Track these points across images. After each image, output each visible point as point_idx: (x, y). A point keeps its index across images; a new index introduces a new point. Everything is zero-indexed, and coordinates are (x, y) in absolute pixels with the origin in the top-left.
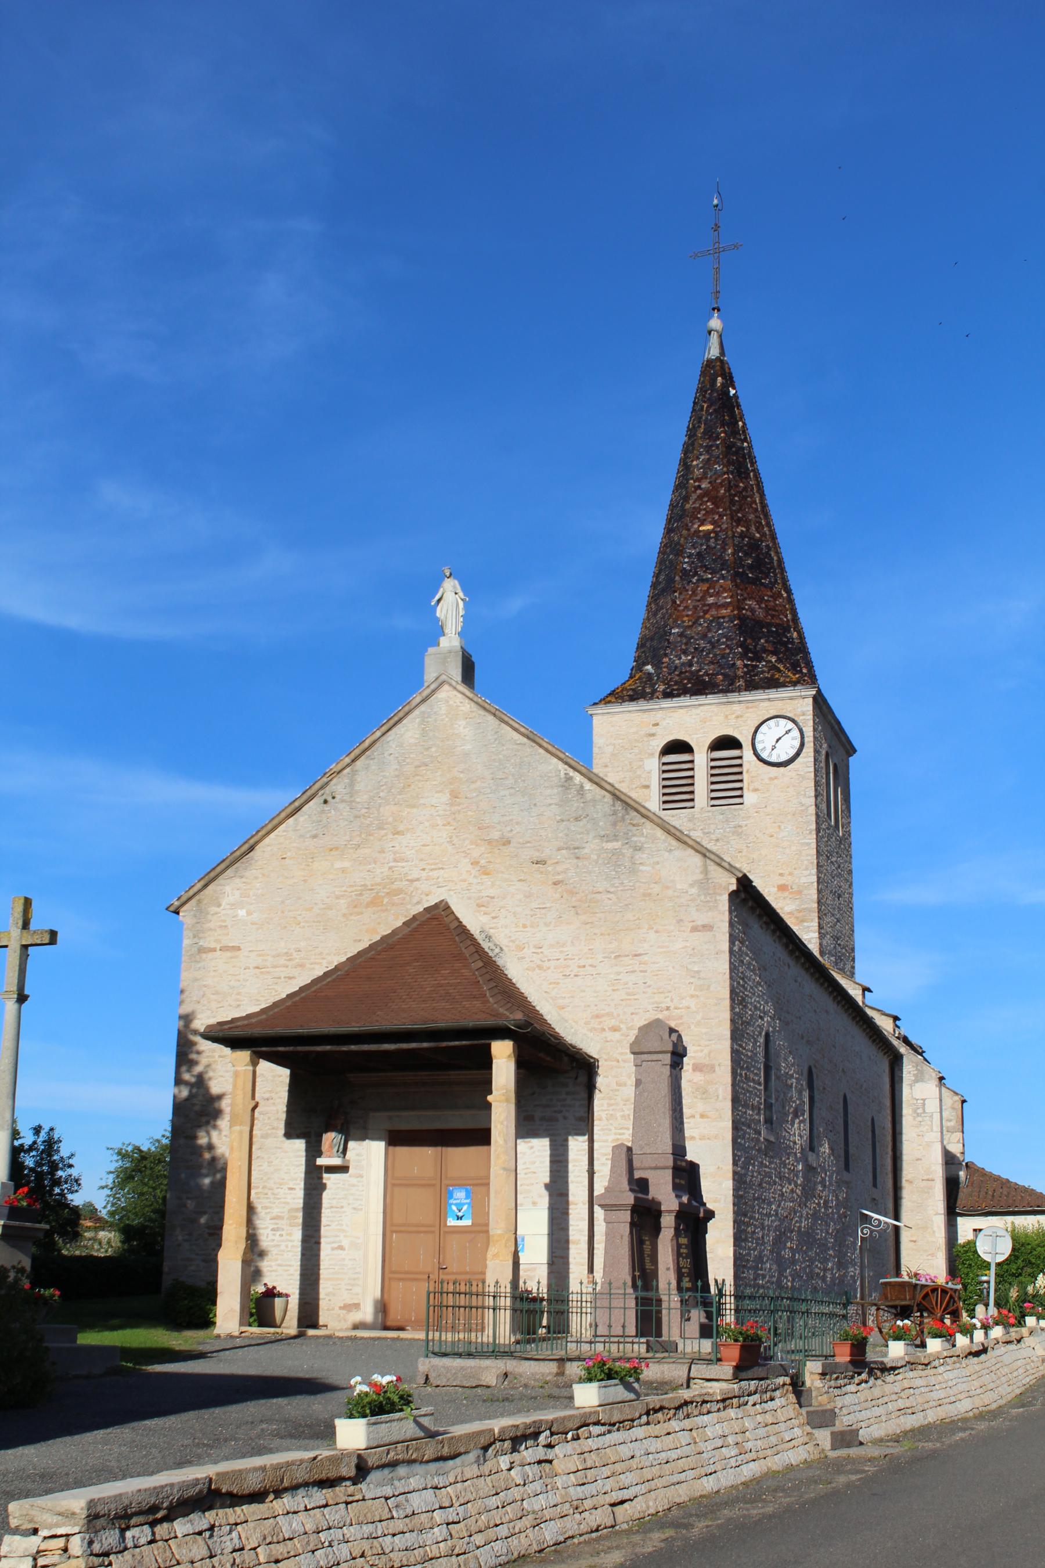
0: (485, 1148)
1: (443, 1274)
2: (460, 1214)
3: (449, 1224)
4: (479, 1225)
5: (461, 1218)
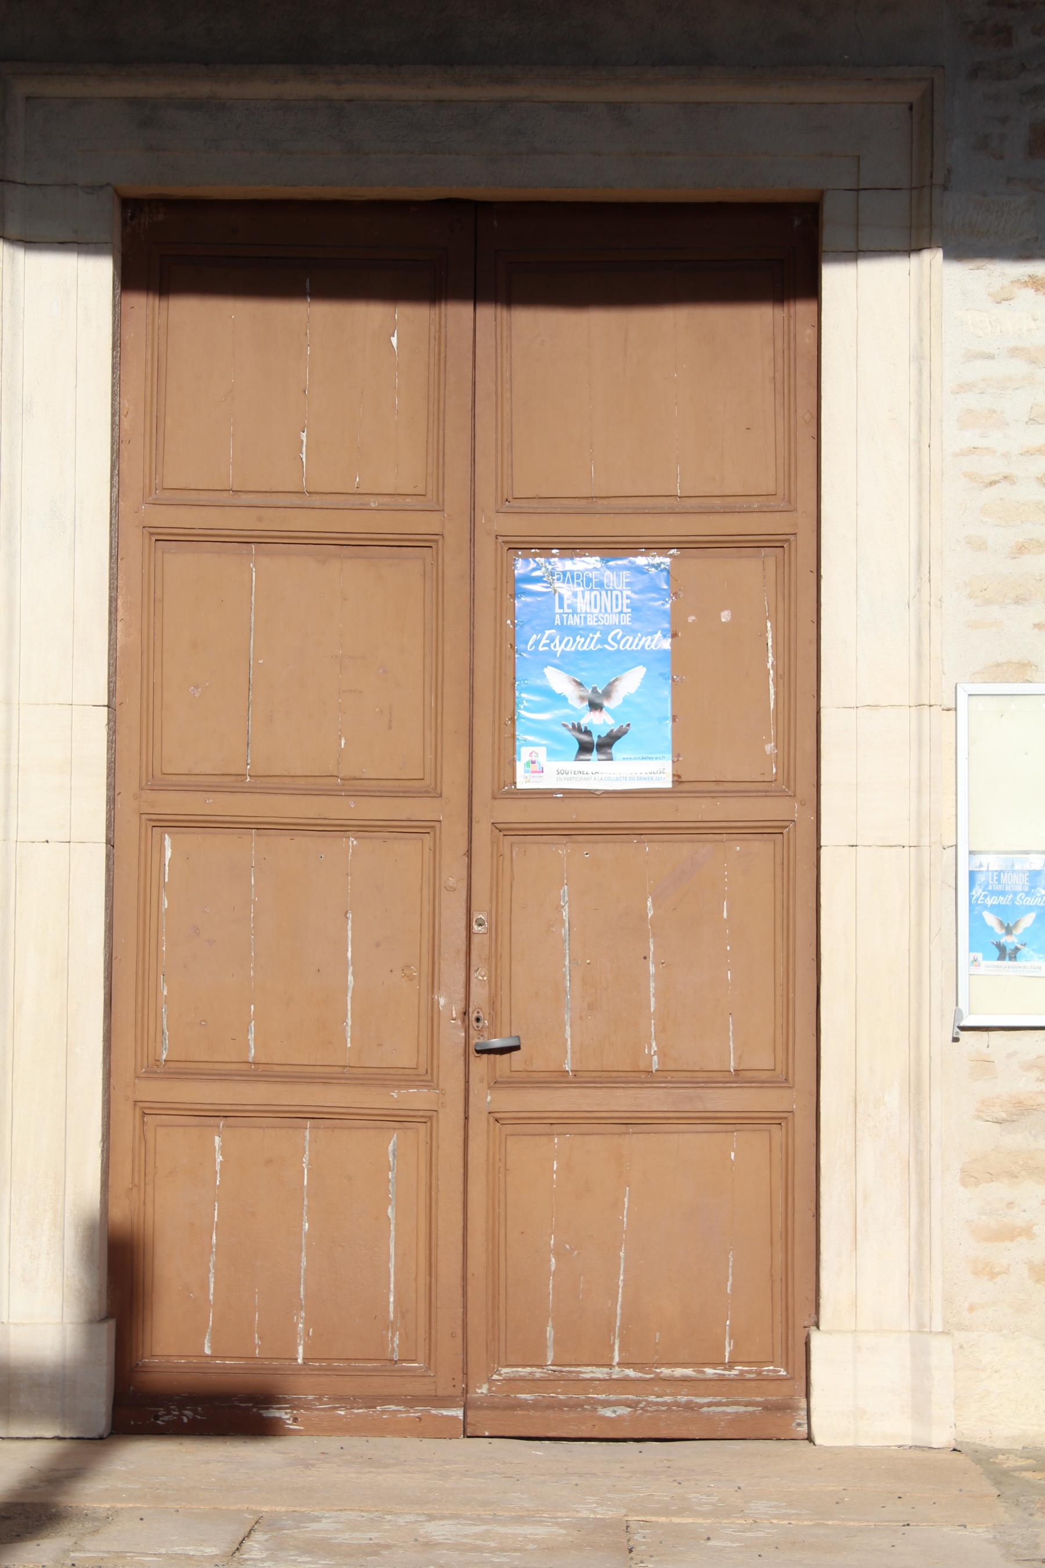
0: (802, 309)
1: (496, 1084)
2: (600, 723)
3: (523, 782)
4: (718, 789)
5: (606, 745)
